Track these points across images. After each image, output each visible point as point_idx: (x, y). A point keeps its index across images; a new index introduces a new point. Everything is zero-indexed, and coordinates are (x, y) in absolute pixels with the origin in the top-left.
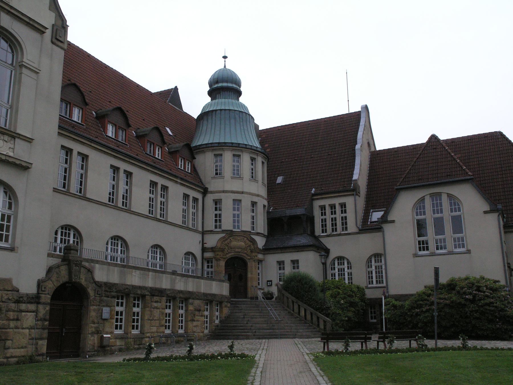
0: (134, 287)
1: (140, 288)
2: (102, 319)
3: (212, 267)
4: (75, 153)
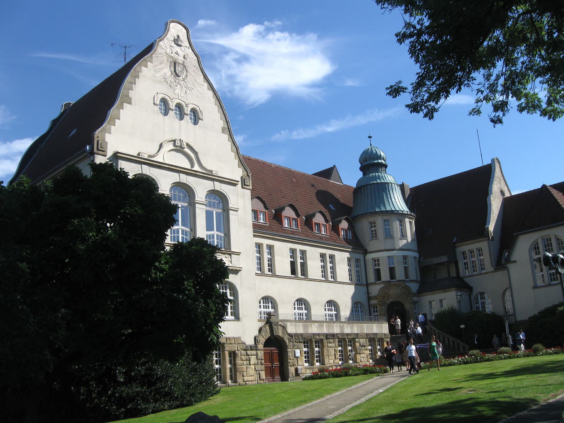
0: (314, 334)
1: (318, 334)
2: (295, 357)
3: (377, 312)
4: (265, 246)
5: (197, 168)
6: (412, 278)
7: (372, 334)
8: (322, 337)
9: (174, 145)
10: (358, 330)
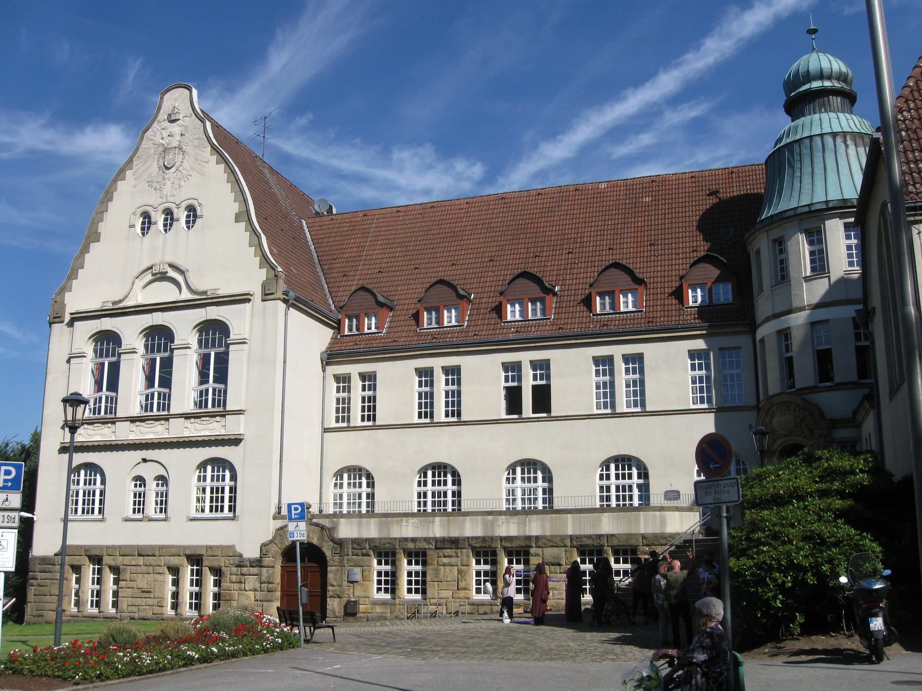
1: (414, 540)
5: (186, 295)
6: (838, 379)
7: (589, 537)
8: (424, 545)
9: (153, 275)
10: (519, 530)
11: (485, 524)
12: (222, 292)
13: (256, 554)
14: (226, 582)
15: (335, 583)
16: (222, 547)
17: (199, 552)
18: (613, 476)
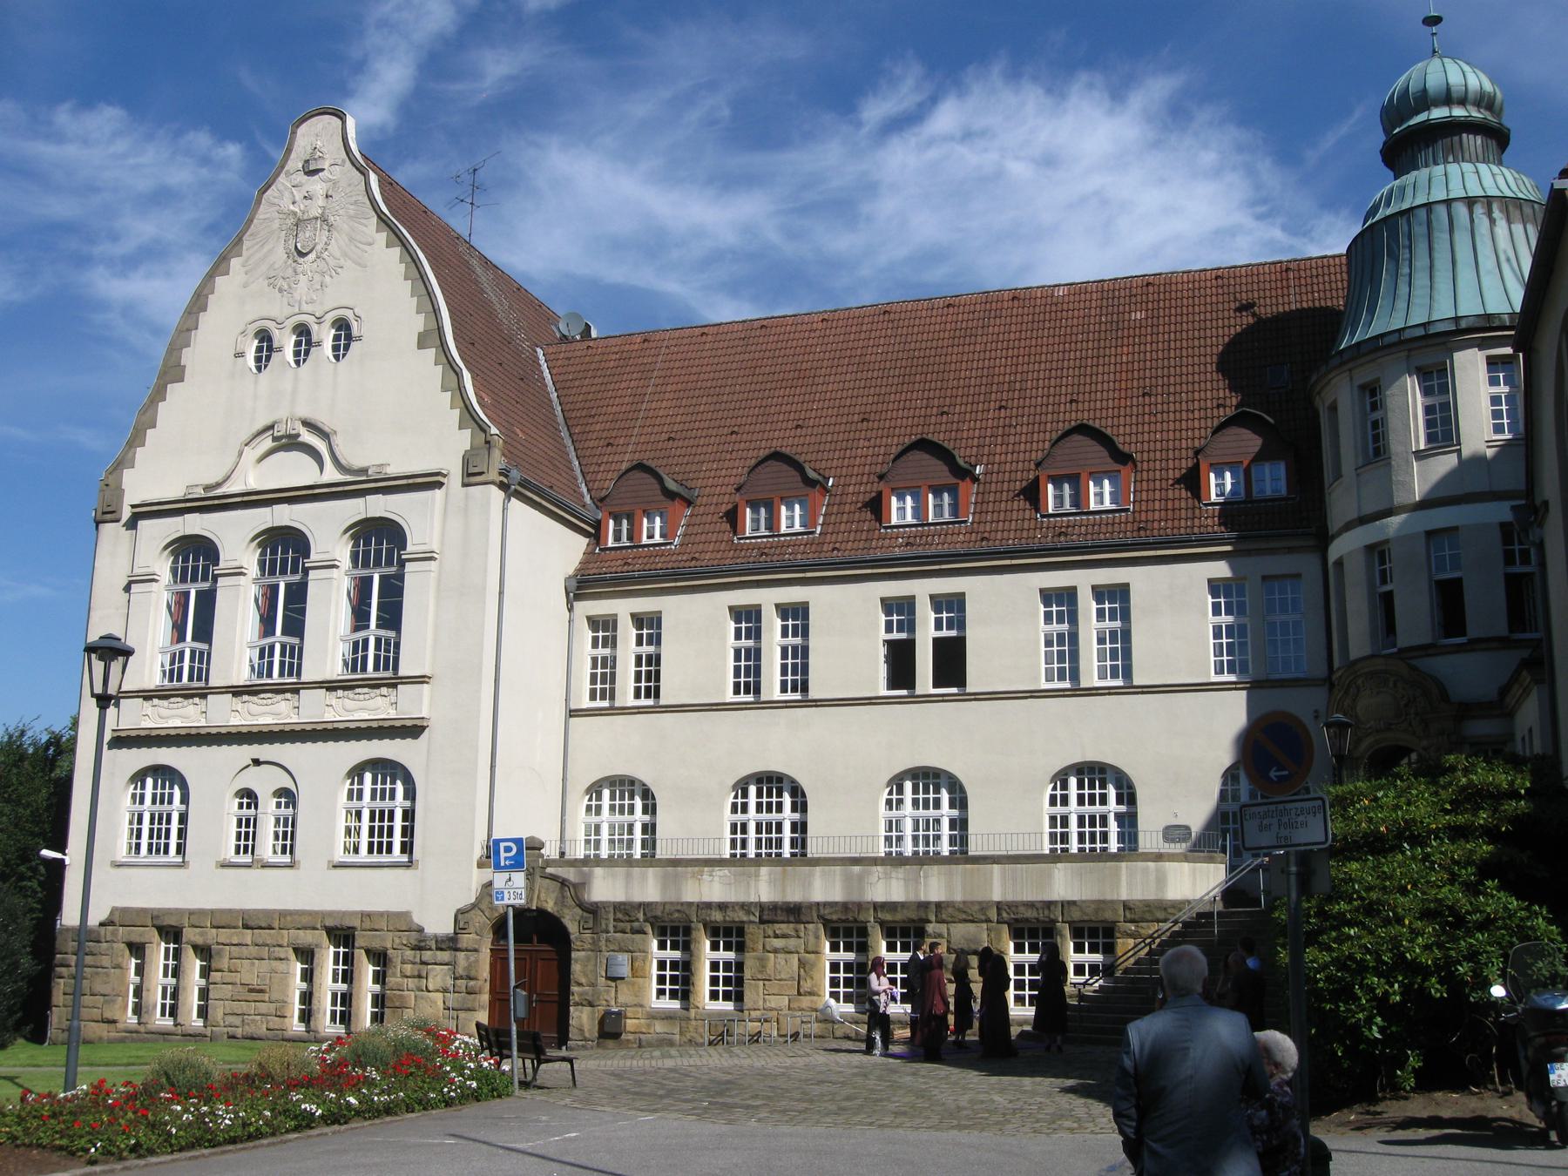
1: (722, 907)
5: (331, 475)
6: (1473, 631)
7: (1031, 905)
9: (275, 439)
11: (848, 879)
12: (392, 470)
13: (445, 927)
14: (394, 975)
15: (583, 981)
16: (389, 915)
17: (348, 923)
18: (1073, 799)
